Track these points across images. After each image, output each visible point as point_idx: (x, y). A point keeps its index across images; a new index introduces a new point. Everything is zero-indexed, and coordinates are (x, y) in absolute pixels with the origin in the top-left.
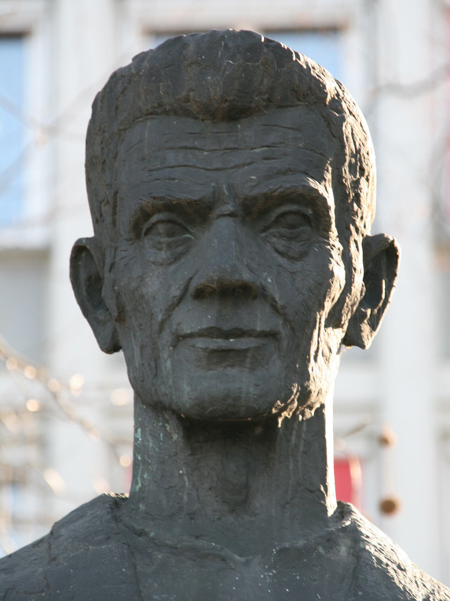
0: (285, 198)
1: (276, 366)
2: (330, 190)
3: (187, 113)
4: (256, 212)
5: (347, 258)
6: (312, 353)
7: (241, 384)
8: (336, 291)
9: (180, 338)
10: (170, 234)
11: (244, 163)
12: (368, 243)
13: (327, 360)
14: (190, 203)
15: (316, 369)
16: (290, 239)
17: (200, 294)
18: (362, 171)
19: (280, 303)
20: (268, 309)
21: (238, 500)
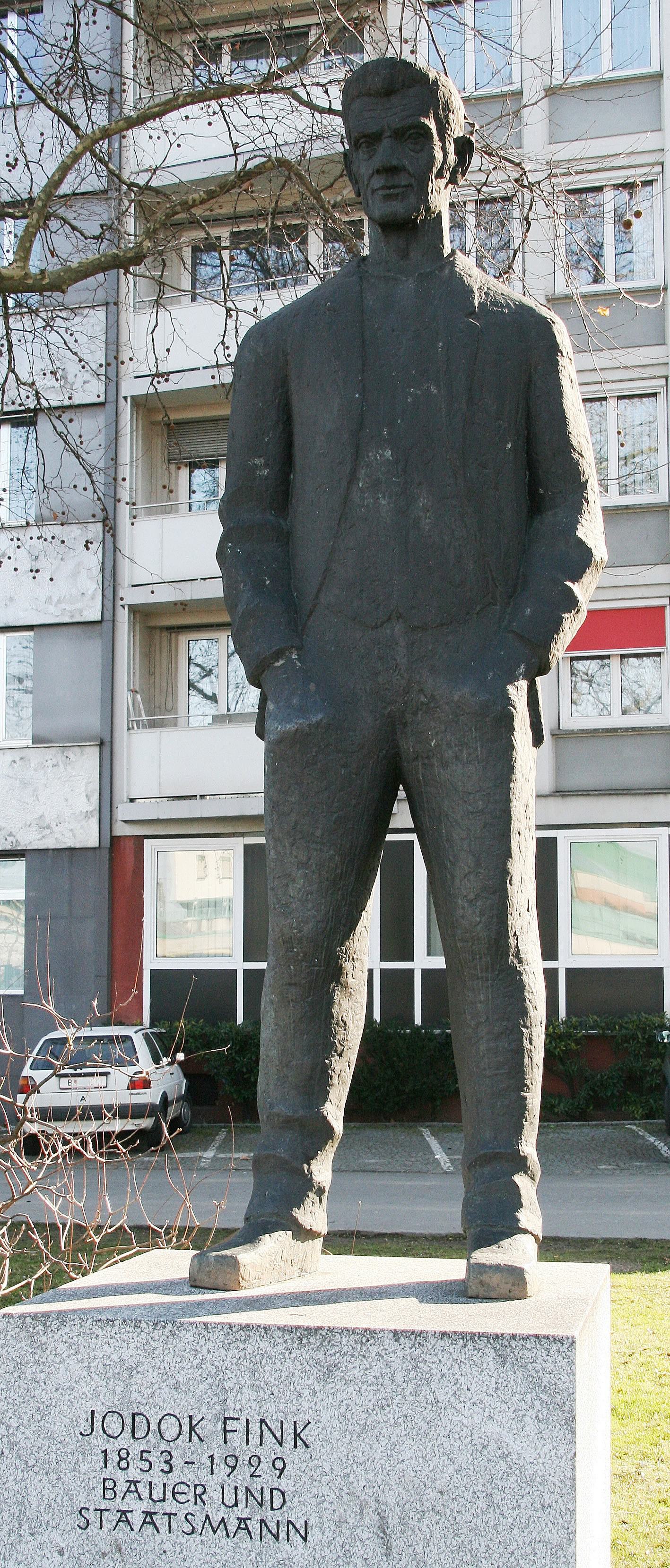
0: (410, 127)
1: (412, 199)
2: (433, 121)
3: (371, 95)
4: (399, 135)
5: (444, 149)
6: (430, 191)
7: (398, 208)
8: (438, 164)
9: (373, 191)
10: (367, 147)
11: (392, 115)
12: (456, 141)
13: (439, 193)
14: (373, 133)
15: (432, 197)
16: (416, 144)
17: (378, 172)
18: (449, 111)
19: (412, 172)
20: (407, 175)
21: (404, 254)
